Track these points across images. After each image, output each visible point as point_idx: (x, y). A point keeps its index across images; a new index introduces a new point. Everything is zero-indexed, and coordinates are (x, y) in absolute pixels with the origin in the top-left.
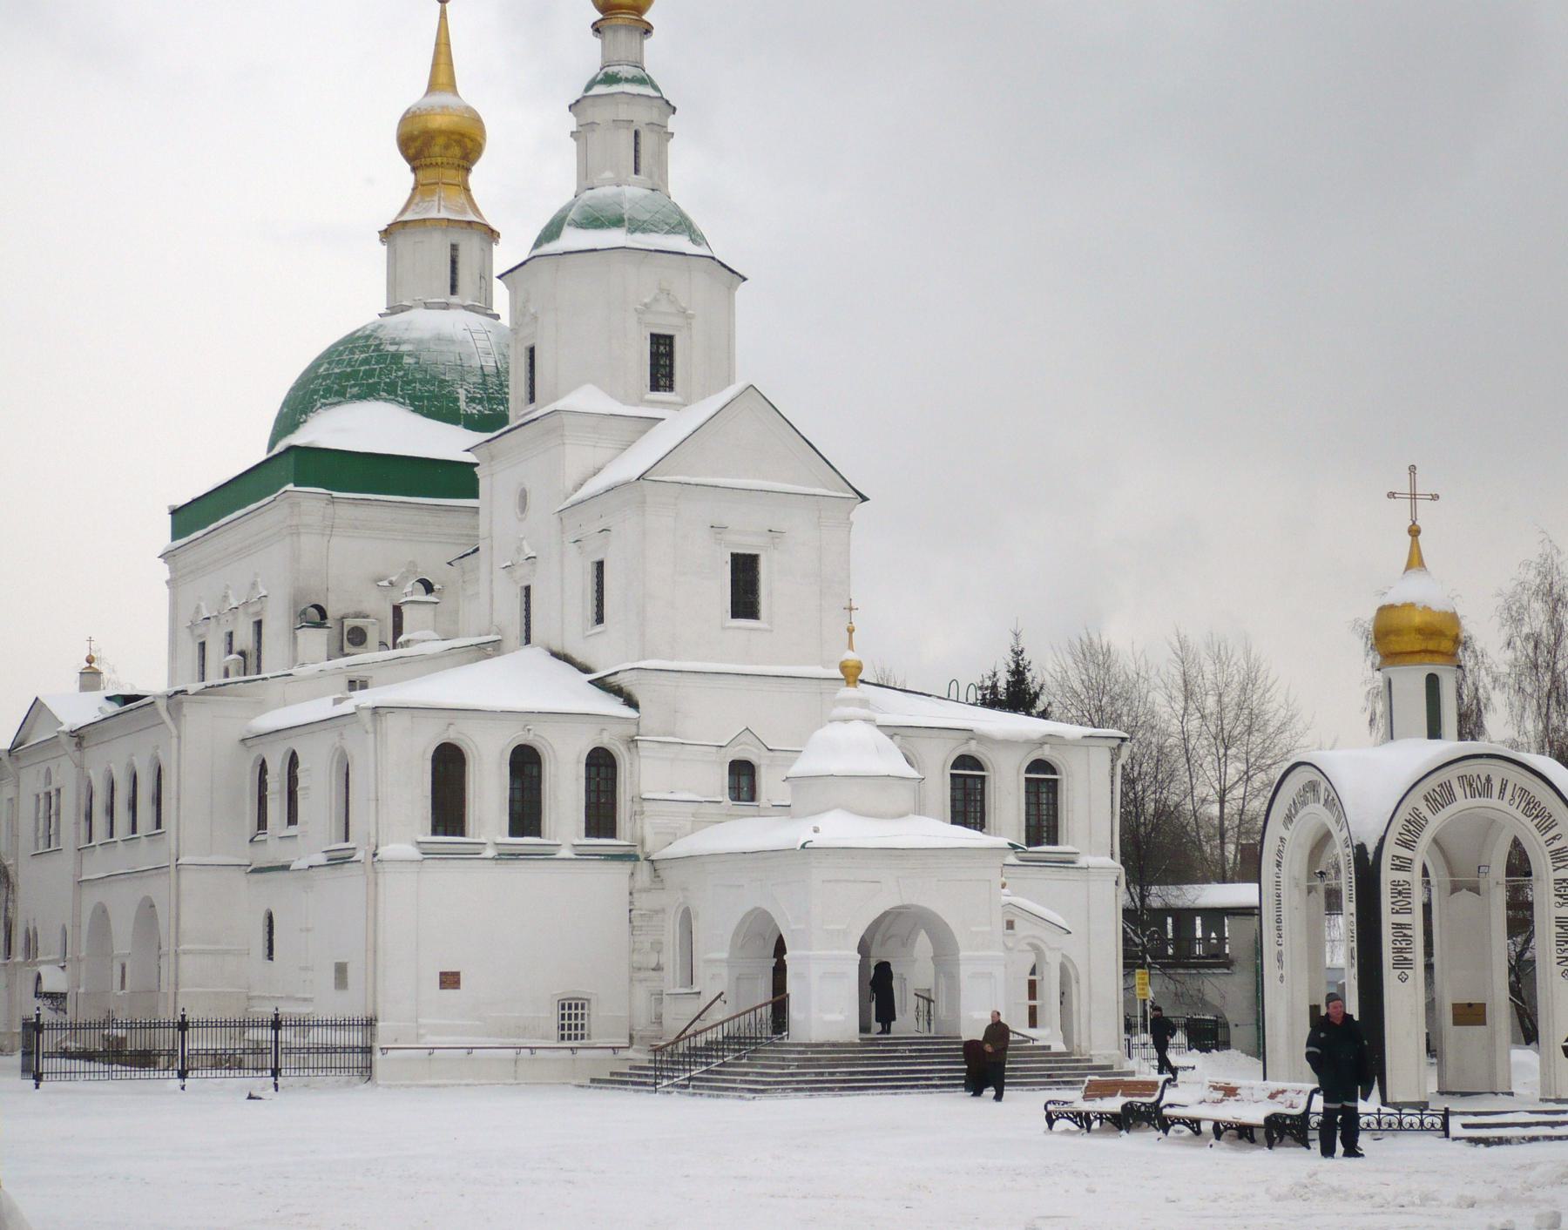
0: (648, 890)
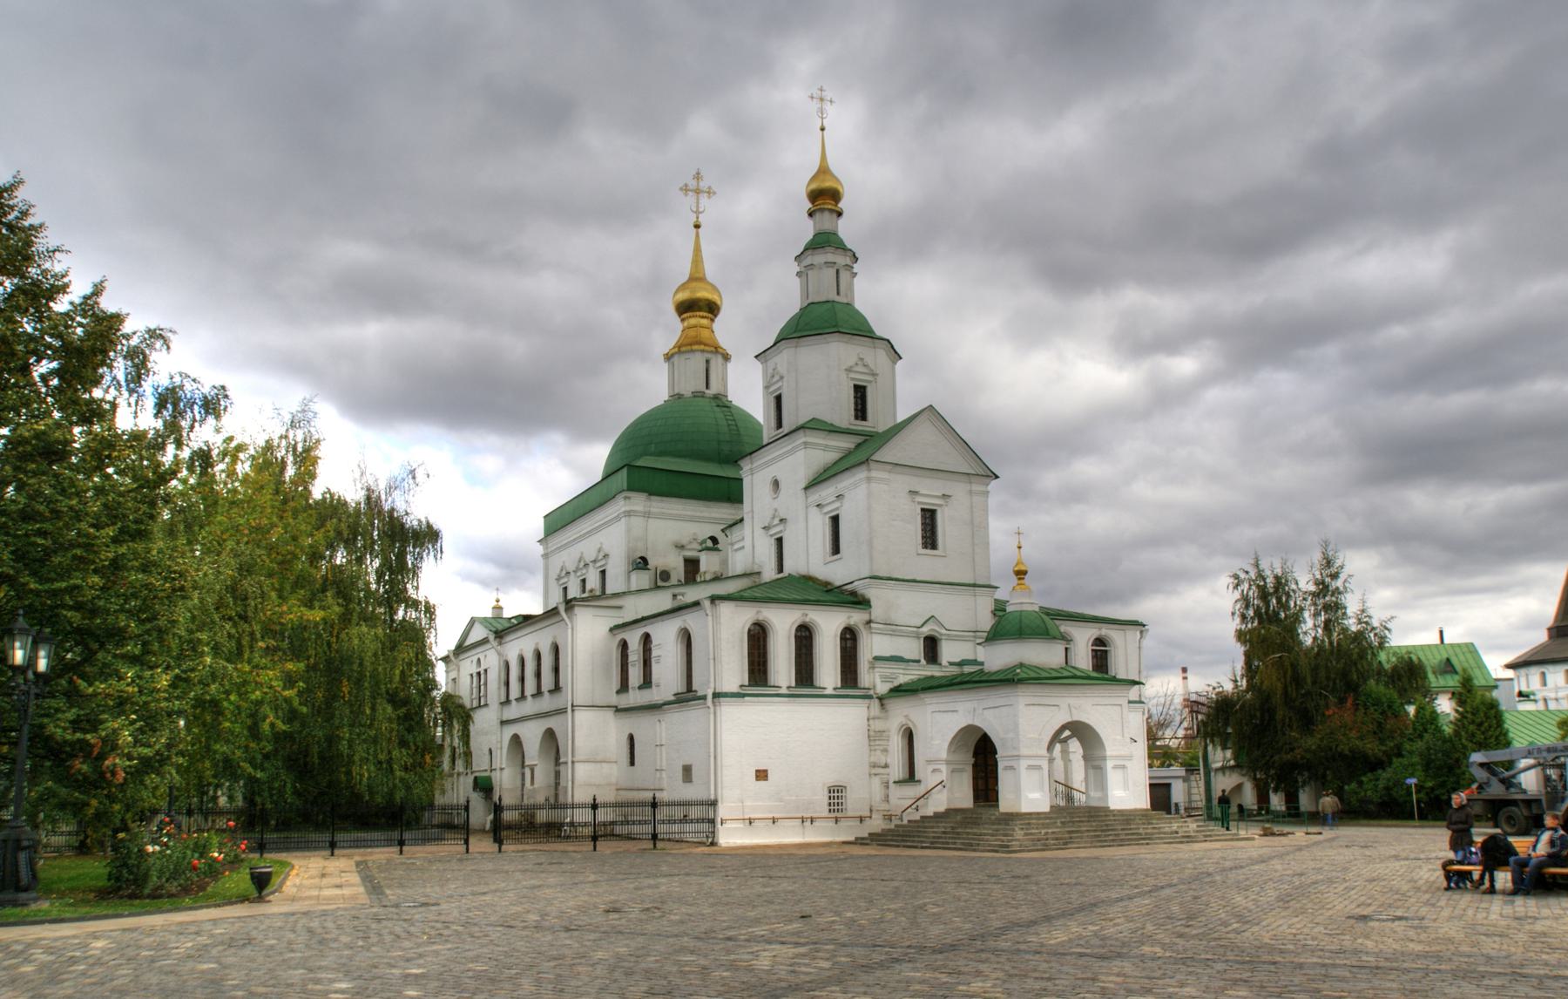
0: (878, 718)
